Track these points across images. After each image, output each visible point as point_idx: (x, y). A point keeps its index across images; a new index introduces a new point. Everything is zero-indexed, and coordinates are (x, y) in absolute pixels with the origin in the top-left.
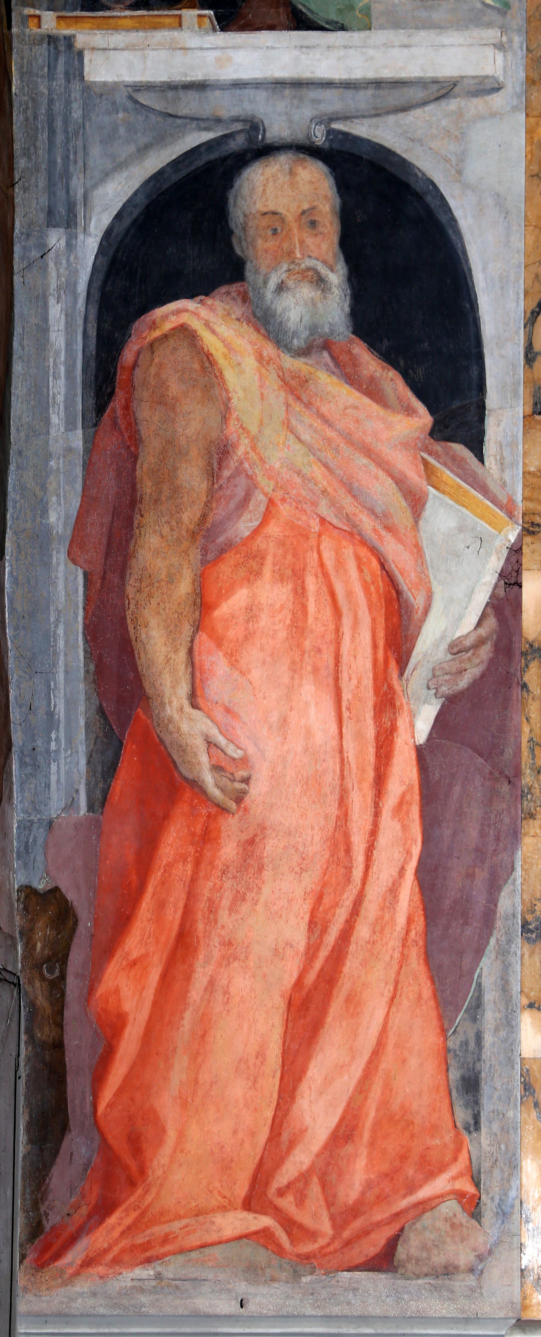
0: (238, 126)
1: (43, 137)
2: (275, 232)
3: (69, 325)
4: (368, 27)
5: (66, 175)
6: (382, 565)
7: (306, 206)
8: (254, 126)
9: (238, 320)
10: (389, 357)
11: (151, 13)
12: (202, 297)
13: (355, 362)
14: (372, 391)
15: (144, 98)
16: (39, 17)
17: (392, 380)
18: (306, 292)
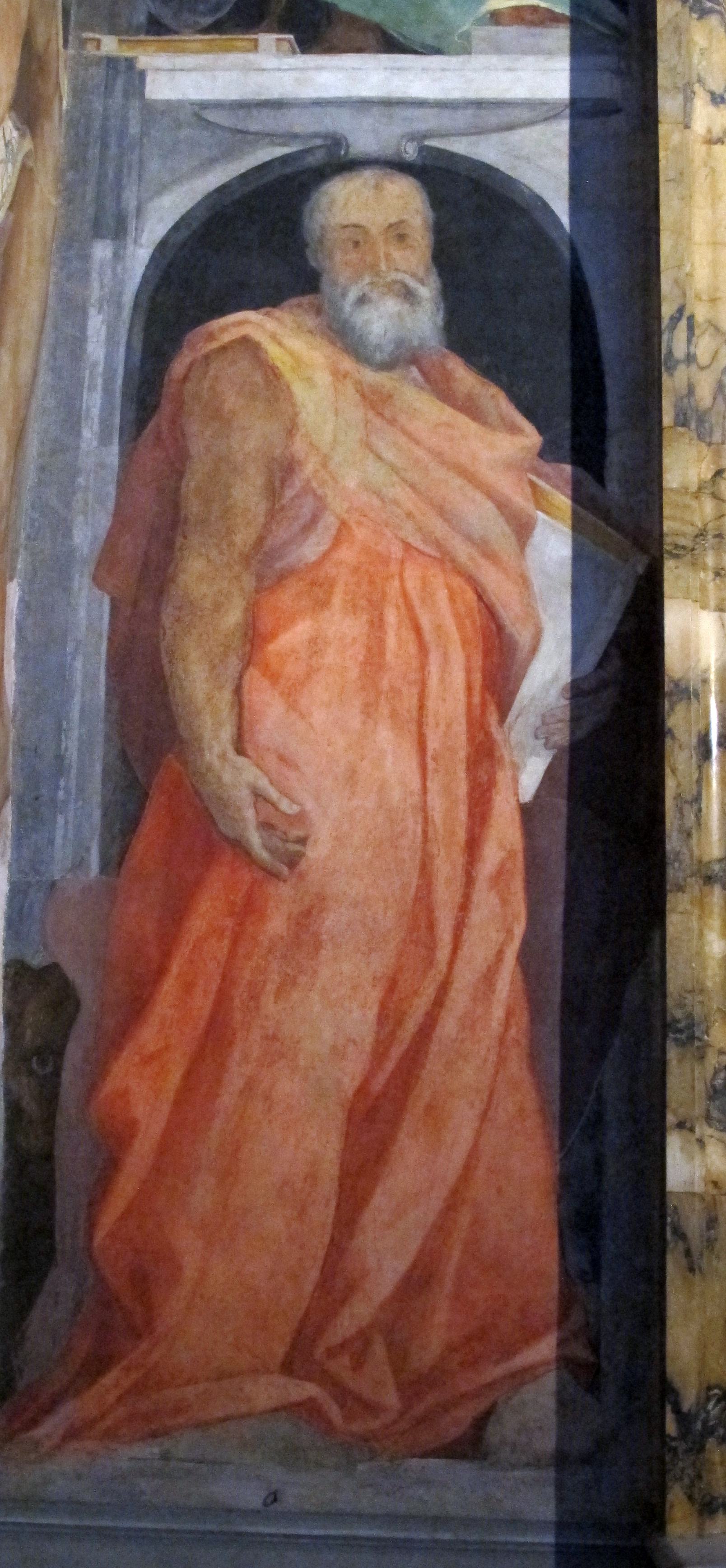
0: (319, 142)
1: (94, 152)
2: (357, 244)
3: (111, 339)
4: (466, 50)
5: (119, 186)
6: (480, 597)
7: (393, 219)
8: (335, 142)
9: (310, 332)
10: (489, 372)
11: (224, 37)
12: (268, 309)
13: (448, 377)
14: (470, 408)
15: (211, 116)
16: (99, 41)
17: (493, 396)
18: (392, 305)
